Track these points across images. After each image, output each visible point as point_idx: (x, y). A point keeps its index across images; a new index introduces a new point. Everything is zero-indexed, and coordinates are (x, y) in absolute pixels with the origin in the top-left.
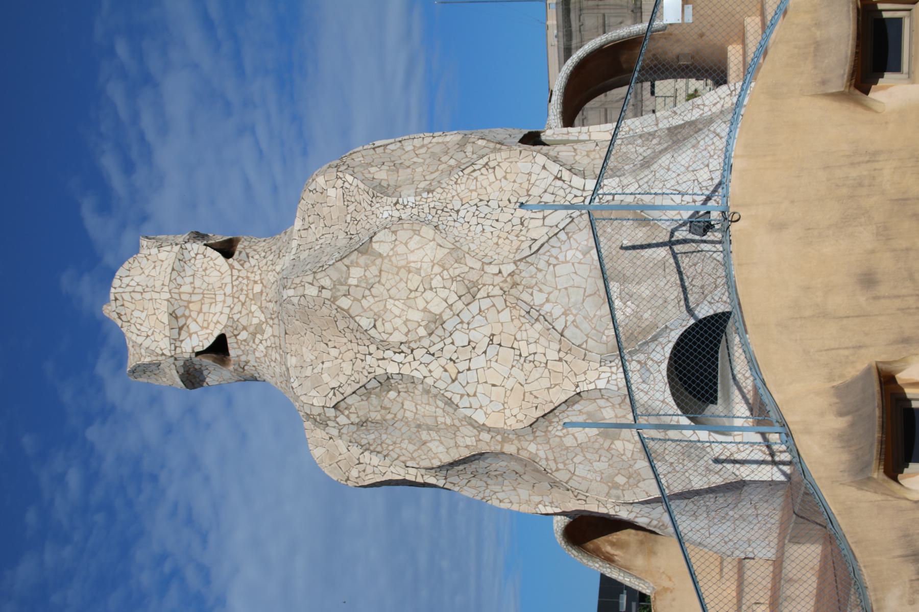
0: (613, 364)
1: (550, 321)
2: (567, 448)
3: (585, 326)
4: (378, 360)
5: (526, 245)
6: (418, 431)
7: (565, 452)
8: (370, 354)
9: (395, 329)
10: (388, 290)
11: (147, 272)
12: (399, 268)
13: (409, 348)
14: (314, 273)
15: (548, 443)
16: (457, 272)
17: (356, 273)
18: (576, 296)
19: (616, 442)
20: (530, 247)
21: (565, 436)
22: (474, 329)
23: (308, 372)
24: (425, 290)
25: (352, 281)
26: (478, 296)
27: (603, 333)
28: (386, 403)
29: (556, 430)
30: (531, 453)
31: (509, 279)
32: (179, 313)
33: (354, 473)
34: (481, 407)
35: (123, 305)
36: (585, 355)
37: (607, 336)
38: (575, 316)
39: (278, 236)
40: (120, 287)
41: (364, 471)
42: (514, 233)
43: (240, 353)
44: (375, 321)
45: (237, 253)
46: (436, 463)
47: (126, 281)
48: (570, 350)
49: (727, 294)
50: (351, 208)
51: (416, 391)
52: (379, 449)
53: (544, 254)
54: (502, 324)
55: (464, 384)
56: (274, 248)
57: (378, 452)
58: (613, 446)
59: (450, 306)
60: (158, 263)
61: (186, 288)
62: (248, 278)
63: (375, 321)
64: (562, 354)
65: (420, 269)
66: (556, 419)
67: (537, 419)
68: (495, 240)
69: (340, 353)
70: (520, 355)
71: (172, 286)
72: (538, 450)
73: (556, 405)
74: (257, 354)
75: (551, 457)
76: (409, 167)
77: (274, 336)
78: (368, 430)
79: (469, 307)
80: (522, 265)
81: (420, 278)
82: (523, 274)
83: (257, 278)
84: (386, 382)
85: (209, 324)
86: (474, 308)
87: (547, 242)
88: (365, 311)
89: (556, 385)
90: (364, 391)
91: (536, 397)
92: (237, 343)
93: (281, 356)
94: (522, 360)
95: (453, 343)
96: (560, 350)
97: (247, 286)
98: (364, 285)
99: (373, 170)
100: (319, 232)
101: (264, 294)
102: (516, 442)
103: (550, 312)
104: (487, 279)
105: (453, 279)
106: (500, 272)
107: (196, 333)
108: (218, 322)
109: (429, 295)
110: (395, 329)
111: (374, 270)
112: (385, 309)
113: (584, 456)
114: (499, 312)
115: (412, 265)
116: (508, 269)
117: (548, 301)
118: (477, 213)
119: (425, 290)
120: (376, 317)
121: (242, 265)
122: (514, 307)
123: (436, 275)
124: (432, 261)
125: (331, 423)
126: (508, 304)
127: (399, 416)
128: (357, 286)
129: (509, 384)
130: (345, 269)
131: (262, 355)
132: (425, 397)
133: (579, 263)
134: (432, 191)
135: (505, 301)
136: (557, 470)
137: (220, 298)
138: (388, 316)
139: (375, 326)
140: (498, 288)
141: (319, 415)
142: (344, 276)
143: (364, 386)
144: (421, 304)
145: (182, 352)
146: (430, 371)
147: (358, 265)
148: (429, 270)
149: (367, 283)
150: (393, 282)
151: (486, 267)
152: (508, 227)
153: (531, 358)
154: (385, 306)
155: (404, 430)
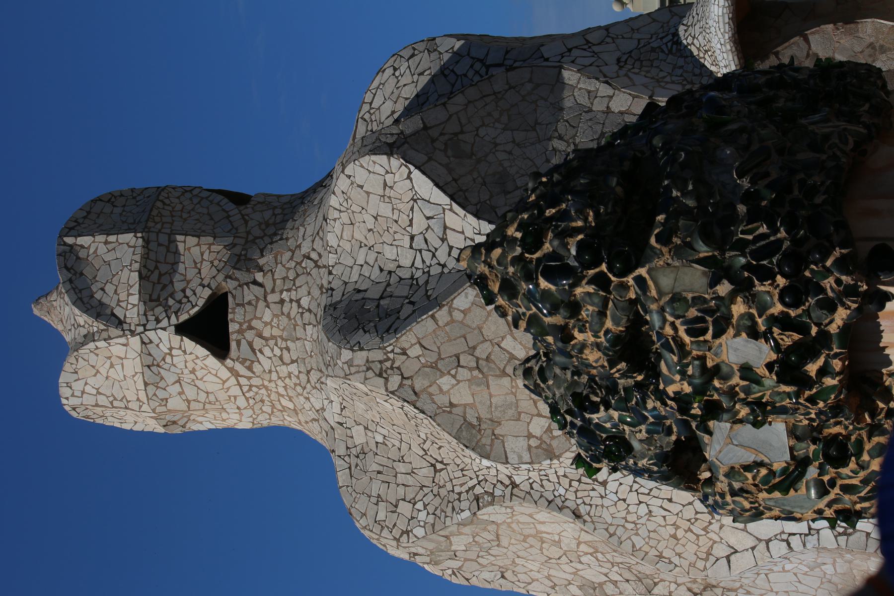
11: (103, 371)
40: (73, 395)
45: (233, 345)
61: (176, 403)
62: (266, 388)
65: (559, 541)
76: (504, 374)
83: (281, 390)
97: (269, 396)
99: (445, 382)
115: (544, 535)
118: (636, 486)
121: (250, 368)
134: (558, 457)
139: (503, 577)
140: (683, 588)
152: (689, 513)
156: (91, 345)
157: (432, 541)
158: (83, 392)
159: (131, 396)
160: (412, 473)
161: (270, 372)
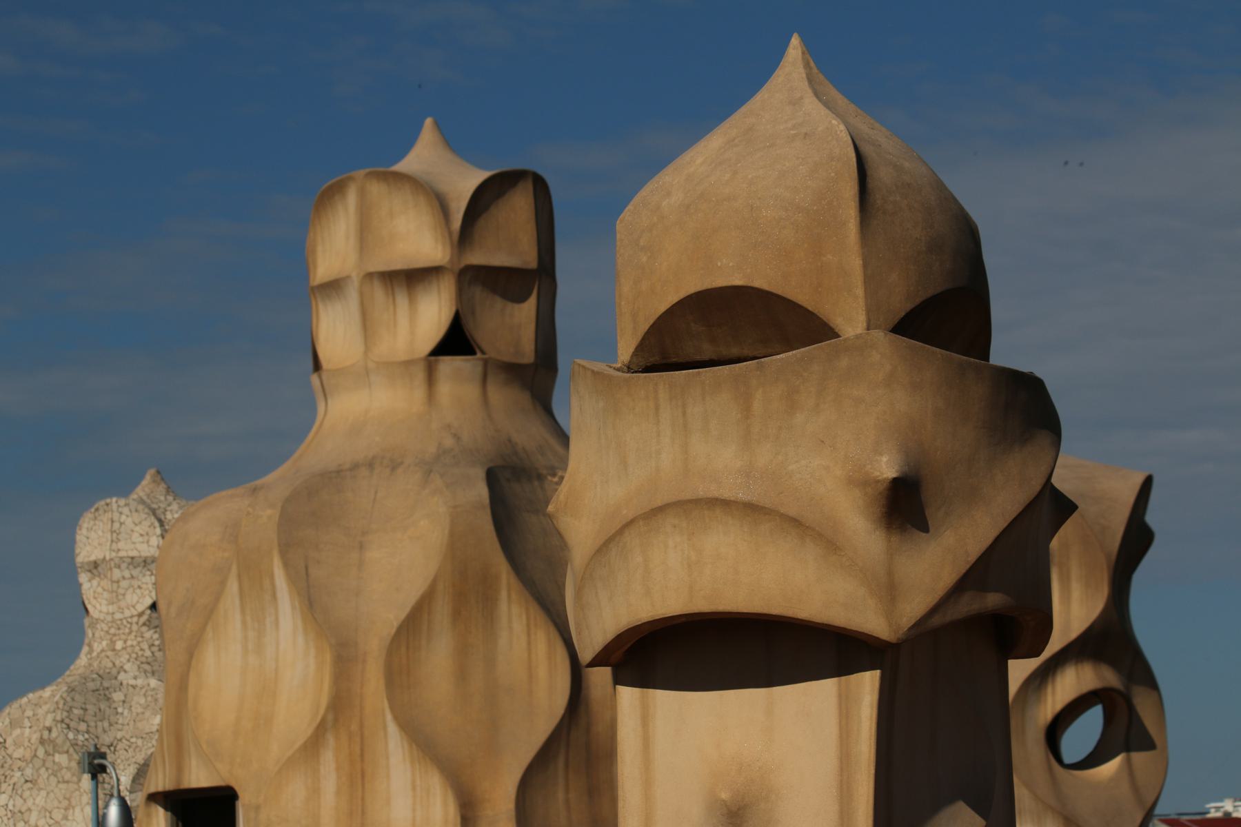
11: (137, 529)
12: (69, 800)
17: (61, 759)
23: (29, 713)
25: (57, 757)
47: (126, 510)
50: (140, 742)
60: (146, 538)
61: (117, 573)
62: (130, 633)
71: (117, 561)
83: (129, 643)
111: (68, 776)
112: (40, 789)
121: (144, 624)
137: (111, 609)
138: (35, 792)
147: (70, 760)
156: (157, 524)
159: (121, 545)
160: (105, 731)
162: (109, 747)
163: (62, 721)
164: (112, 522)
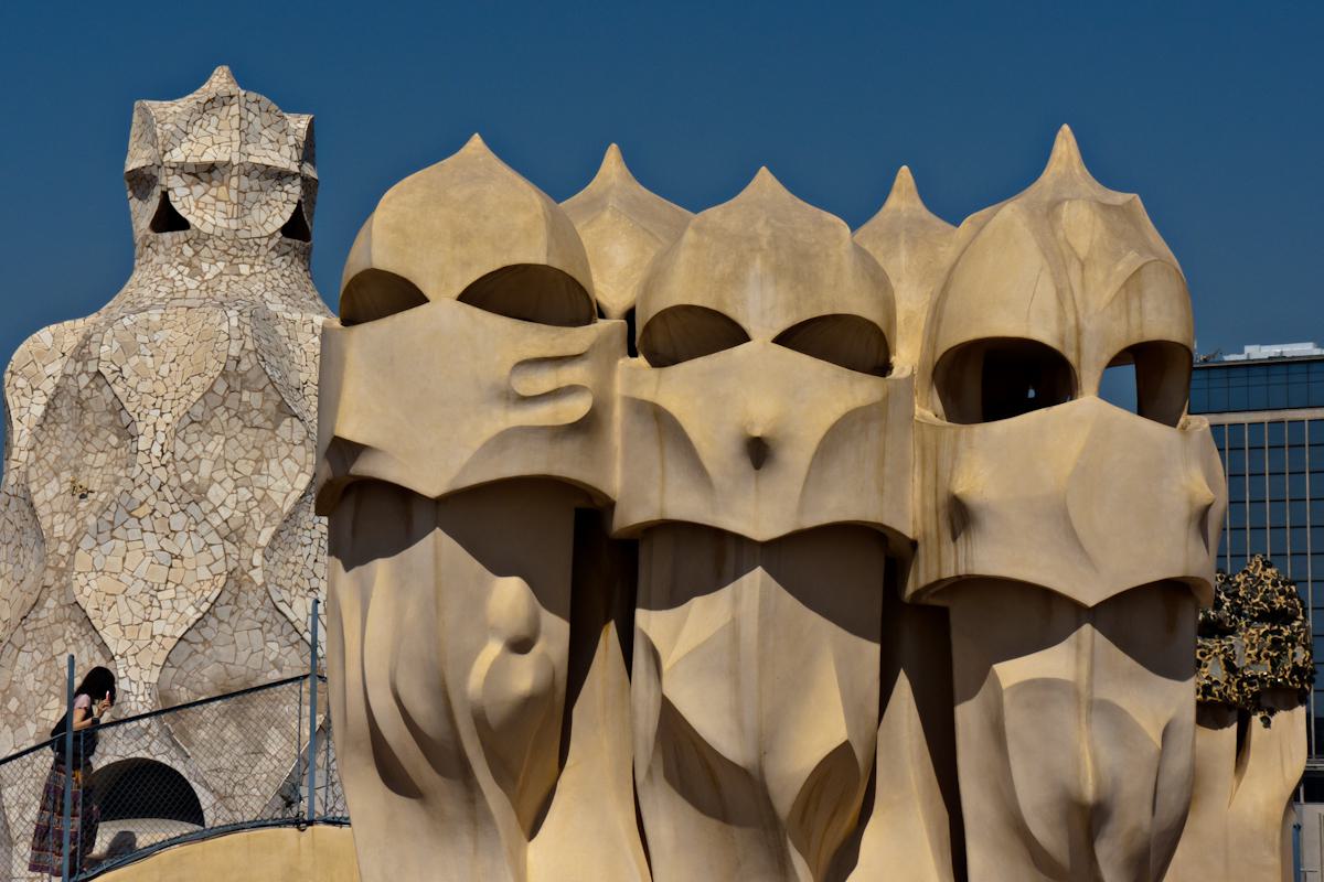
0: (147, 697)
1: (197, 626)
2: (51, 644)
3: (192, 664)
4: (155, 424)
5: (285, 595)
6: (71, 468)
7: (45, 640)
8: (162, 414)
9: (190, 446)
10: (235, 437)
11: (265, 132)
13: (168, 462)
14: (256, 351)
15: (57, 622)
16: (255, 517)
18: (225, 652)
19: (57, 700)
20: (282, 601)
21: (65, 641)
22: (189, 538)
23: (142, 338)
24: (235, 480)
25: (246, 396)
26: (226, 543)
27: (182, 686)
28: (104, 433)
29: (71, 630)
30: (45, 601)
31: (246, 577)
32: (216, 174)
33: (21, 383)
34: (98, 544)
35: (224, 105)
36: (158, 666)
37: (178, 690)
38: (203, 653)
39: (310, 287)
41: (23, 395)
42: (300, 582)
43: (168, 246)
44: (199, 422)
45: (289, 241)
46: (33, 487)
47: (255, 108)
48: (164, 648)
49: (224, 823)
51: (116, 469)
52: (50, 420)
53: (274, 617)
54: (195, 569)
55: (126, 525)
56: (294, 286)
57: (45, 419)
58: (52, 697)
59: (215, 510)
62: (258, 256)
63: (199, 422)
64: (159, 639)
66: (84, 632)
67: (84, 611)
68: (292, 559)
69: (164, 378)
70: (158, 591)
72: (49, 609)
73: (101, 632)
74: (166, 266)
75: (40, 624)
77: (186, 291)
78: (71, 409)
79: (214, 532)
80: (261, 592)
81: (249, 474)
82: (251, 594)
83: (257, 269)
84: (127, 433)
85: (201, 209)
86: (213, 538)
87: (288, 620)
88: (211, 410)
89: (124, 631)
90: (117, 408)
91: (110, 609)
92: (179, 243)
93: (162, 299)
94: (153, 593)
95: (173, 512)
96: (164, 636)
97: (248, 256)
98: (241, 409)
100: (309, 347)
101: (236, 278)
102: (58, 584)
103: (207, 625)
104: (246, 553)
105: (247, 512)
106: (254, 567)
107: (191, 194)
108: (204, 221)
109: (229, 484)
110: (190, 446)
111: (259, 420)
113: (41, 663)
114: (208, 566)
115: (265, 465)
116: (258, 576)
117: (220, 622)
119: (235, 480)
120: (204, 423)
121: (273, 249)
122: (213, 584)
123: (252, 492)
124: (268, 488)
125: (80, 365)
126: (217, 577)
127: (89, 447)
128: (240, 401)
129: (125, 577)
130: (261, 387)
131: (165, 273)
132: (111, 479)
133: (264, 657)
135: (221, 574)
136: (25, 632)
138: (204, 436)
139: (193, 422)
140: (236, 564)
141: (90, 353)
142: (253, 386)
143: (123, 408)
144: (219, 476)
145: (167, 176)
146: (140, 486)
147: (264, 401)
148: (258, 485)
149: (244, 413)
150: (244, 442)
151: (260, 551)
152: (307, 574)
153: (155, 603)
154: (217, 433)
155: (73, 452)
157: (260, 377)
158: (249, 110)
159: (250, 148)
161: (272, 264)
162: (298, 389)
163: (256, 351)
164: (241, 119)
